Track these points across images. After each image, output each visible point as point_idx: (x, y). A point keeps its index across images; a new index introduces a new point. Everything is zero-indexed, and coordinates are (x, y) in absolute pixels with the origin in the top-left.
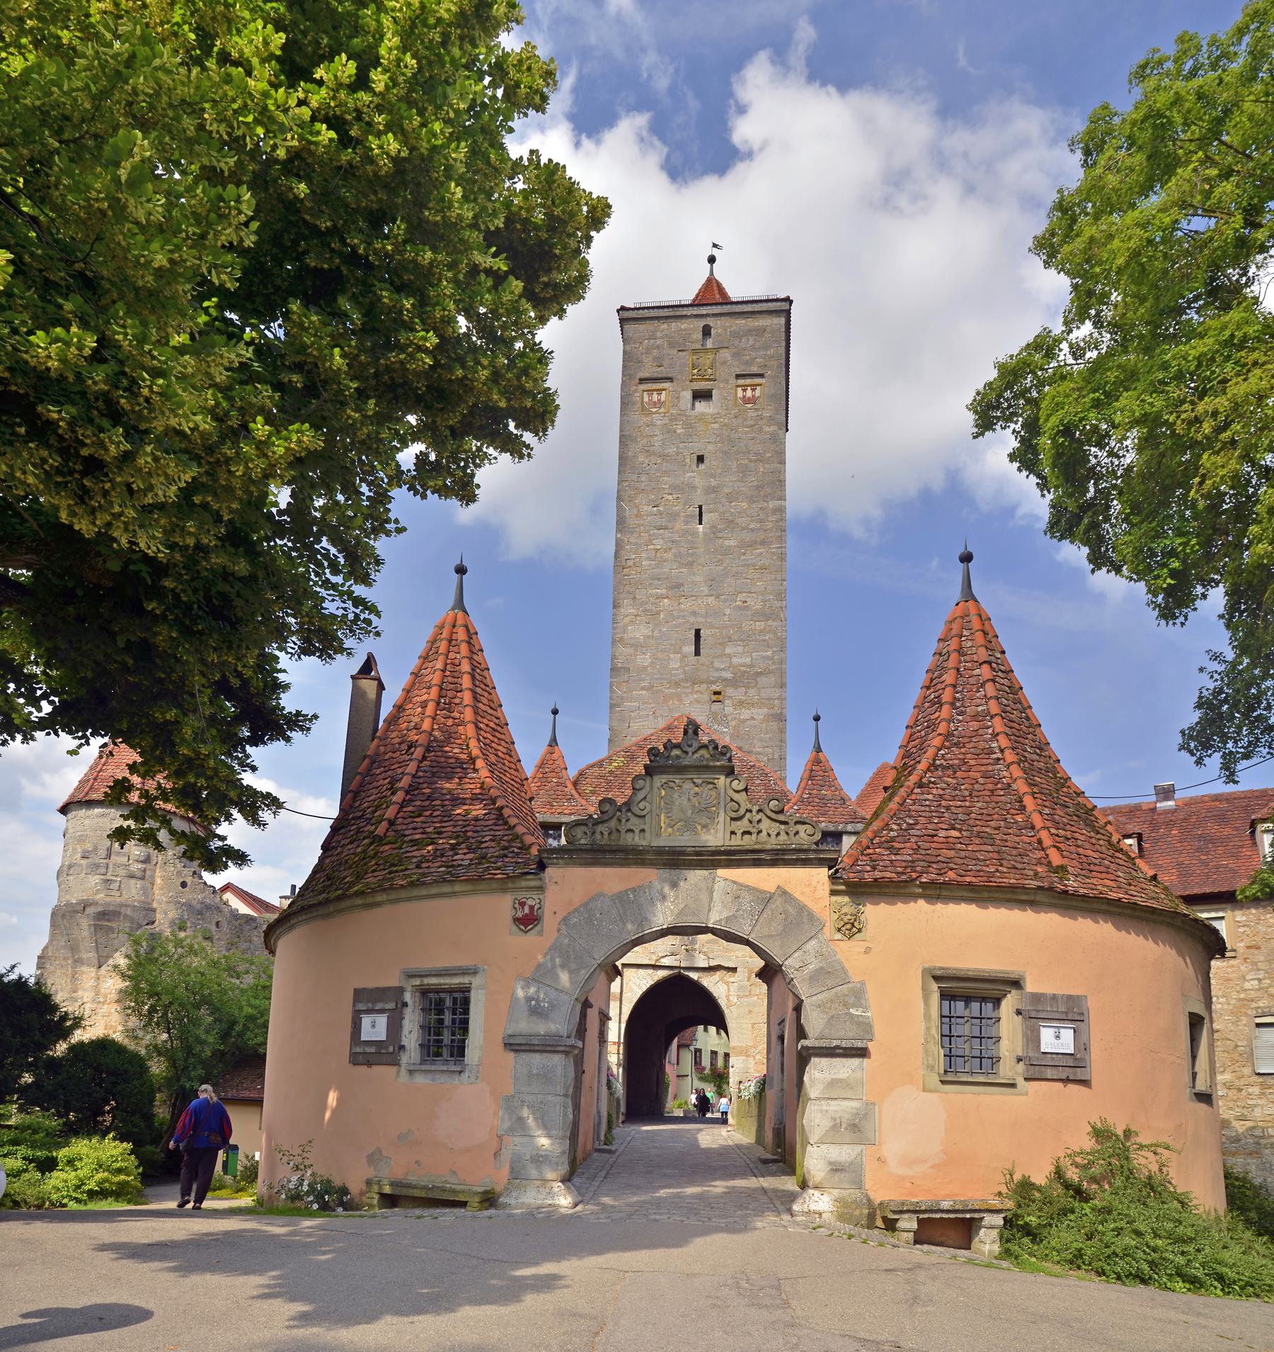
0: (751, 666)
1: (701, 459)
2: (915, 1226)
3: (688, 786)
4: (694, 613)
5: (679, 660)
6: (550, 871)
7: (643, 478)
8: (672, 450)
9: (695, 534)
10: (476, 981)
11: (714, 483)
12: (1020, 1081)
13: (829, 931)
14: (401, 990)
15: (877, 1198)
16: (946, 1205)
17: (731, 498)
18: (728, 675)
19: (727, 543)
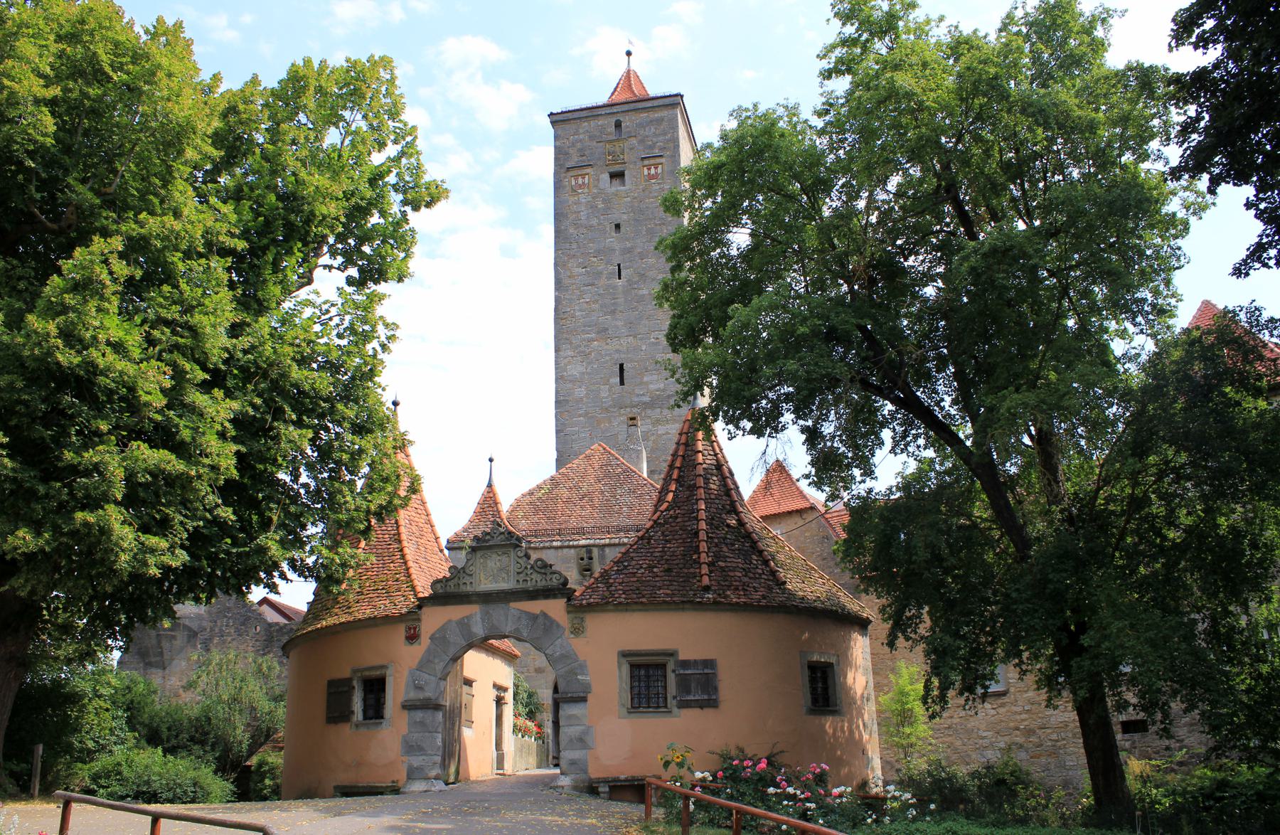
0: (664, 390)
1: (618, 226)
2: (607, 789)
3: (494, 556)
4: (618, 351)
5: (608, 389)
6: (424, 609)
7: (574, 246)
8: (594, 222)
9: (615, 287)
10: (388, 673)
11: (628, 245)
12: (675, 710)
13: (567, 632)
14: (350, 680)
15: (593, 776)
16: (622, 777)
17: (642, 256)
18: (646, 399)
19: (641, 292)
